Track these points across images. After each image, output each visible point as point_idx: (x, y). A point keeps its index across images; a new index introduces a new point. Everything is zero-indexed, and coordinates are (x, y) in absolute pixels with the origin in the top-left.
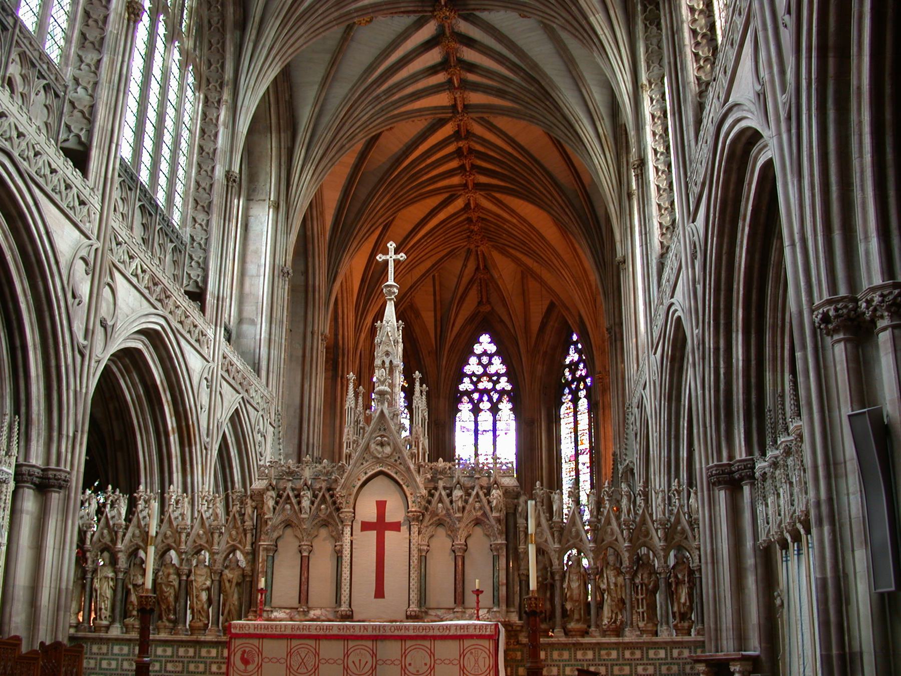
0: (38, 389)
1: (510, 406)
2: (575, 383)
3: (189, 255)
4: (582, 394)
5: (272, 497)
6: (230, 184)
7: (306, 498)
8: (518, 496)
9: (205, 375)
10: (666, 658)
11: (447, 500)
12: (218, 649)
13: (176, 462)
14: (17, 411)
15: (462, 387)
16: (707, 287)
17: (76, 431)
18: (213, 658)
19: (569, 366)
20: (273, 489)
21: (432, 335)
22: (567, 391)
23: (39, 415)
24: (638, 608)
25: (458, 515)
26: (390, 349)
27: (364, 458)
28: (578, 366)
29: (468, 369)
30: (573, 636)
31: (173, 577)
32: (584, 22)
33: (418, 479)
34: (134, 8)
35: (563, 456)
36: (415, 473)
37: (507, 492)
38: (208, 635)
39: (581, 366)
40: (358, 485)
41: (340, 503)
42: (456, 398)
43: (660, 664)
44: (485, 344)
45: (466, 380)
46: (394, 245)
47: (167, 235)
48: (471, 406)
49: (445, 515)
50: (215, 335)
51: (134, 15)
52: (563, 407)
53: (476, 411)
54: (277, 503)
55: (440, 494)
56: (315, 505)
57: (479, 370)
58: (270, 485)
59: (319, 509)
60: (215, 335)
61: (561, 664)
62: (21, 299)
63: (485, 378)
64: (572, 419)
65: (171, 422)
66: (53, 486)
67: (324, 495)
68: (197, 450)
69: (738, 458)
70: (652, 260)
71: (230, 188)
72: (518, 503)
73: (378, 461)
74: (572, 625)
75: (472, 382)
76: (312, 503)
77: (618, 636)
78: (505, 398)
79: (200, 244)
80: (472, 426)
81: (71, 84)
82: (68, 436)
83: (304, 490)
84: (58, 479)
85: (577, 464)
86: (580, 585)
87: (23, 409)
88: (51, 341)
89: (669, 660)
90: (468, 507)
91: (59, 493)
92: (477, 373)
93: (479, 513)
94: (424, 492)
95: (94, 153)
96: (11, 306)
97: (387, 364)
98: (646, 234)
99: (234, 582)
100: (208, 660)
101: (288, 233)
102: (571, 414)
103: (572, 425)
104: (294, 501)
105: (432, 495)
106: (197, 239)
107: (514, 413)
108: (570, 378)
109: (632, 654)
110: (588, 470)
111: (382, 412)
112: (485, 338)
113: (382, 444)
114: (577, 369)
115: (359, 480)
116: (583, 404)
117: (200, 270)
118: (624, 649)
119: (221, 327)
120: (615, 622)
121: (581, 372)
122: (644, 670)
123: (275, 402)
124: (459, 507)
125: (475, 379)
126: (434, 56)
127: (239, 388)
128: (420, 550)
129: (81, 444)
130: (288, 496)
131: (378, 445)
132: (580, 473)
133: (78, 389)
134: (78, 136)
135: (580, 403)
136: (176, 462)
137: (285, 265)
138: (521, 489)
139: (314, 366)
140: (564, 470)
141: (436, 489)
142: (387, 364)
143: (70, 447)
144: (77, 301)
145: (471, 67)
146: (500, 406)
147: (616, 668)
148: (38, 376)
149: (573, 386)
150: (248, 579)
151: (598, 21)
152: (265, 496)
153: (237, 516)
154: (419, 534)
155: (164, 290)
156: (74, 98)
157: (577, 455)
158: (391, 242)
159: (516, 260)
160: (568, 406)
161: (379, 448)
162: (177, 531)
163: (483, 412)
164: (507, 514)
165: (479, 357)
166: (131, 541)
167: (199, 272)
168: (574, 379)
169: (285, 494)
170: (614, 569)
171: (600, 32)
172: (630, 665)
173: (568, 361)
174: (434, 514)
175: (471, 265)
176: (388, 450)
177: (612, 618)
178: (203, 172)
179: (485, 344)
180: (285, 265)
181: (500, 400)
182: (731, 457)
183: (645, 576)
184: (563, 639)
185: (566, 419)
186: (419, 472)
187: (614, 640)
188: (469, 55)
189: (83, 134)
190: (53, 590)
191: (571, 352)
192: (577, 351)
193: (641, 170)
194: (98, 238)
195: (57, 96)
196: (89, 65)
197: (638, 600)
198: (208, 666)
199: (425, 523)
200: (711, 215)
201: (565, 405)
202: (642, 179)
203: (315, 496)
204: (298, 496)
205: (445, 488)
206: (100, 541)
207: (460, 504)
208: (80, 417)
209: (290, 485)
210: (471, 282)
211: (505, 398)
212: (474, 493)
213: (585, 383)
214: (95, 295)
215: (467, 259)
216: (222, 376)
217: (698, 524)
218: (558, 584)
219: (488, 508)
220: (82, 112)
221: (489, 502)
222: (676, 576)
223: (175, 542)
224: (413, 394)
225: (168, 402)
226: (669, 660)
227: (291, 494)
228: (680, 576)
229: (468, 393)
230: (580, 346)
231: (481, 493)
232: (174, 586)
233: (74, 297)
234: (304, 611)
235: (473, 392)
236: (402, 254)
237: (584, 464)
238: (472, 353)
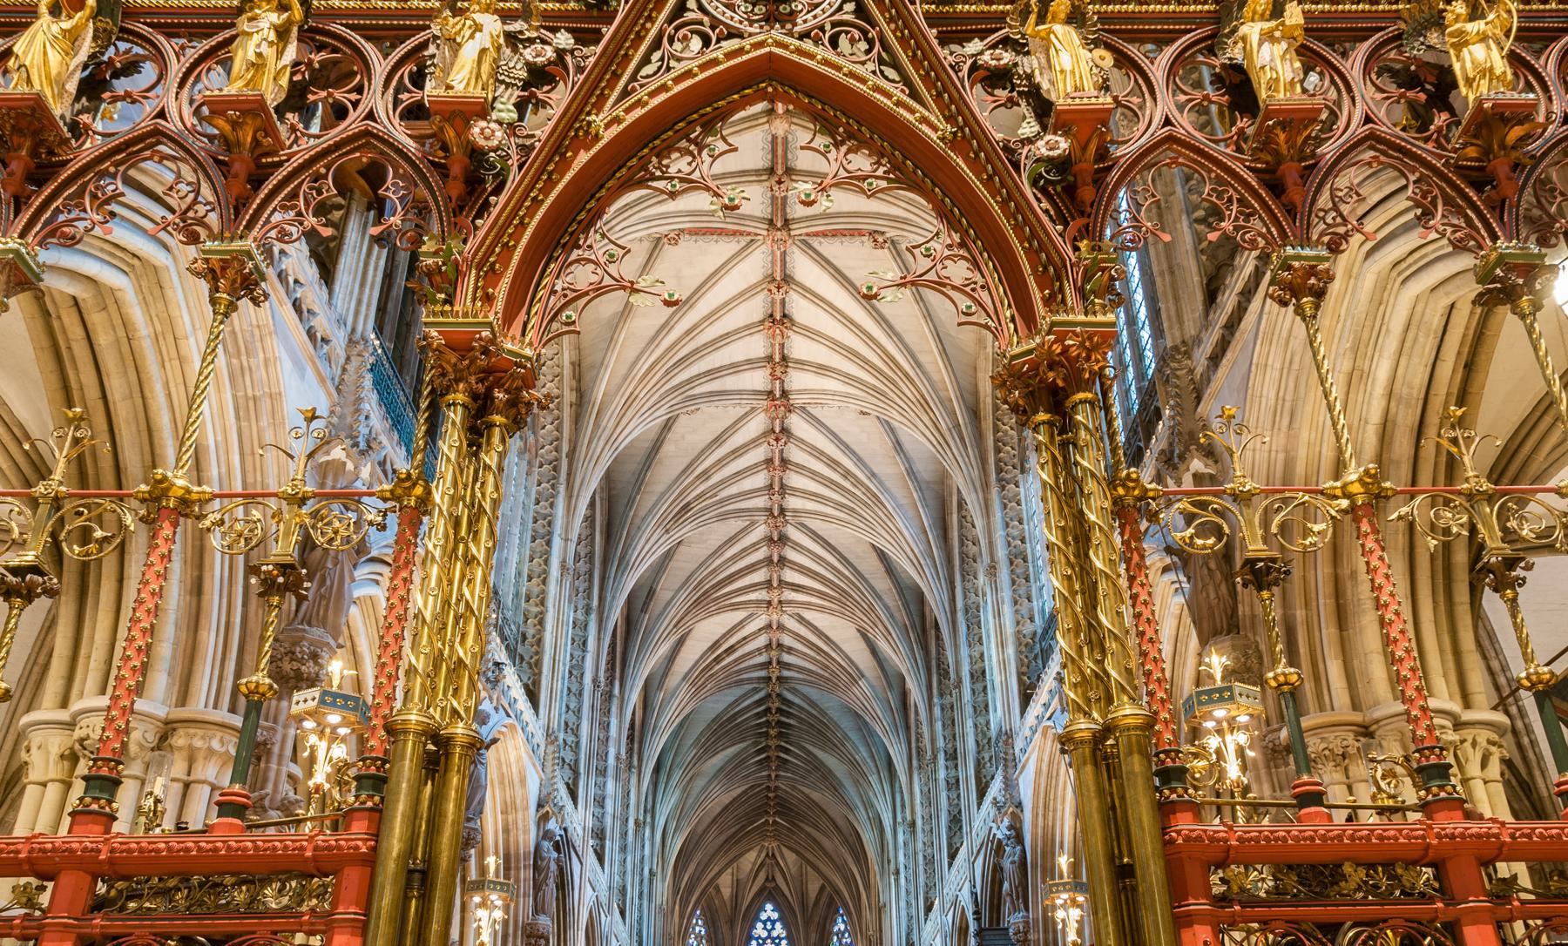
21: (728, 904)
44: (769, 911)
57: (764, 934)
101: (663, 880)
112: (769, 907)
151: (873, 779)
159: (798, 853)
173: (836, 929)
175: (763, 855)
179: (769, 911)
210: (762, 865)
215: (760, 852)
238: (757, 918)
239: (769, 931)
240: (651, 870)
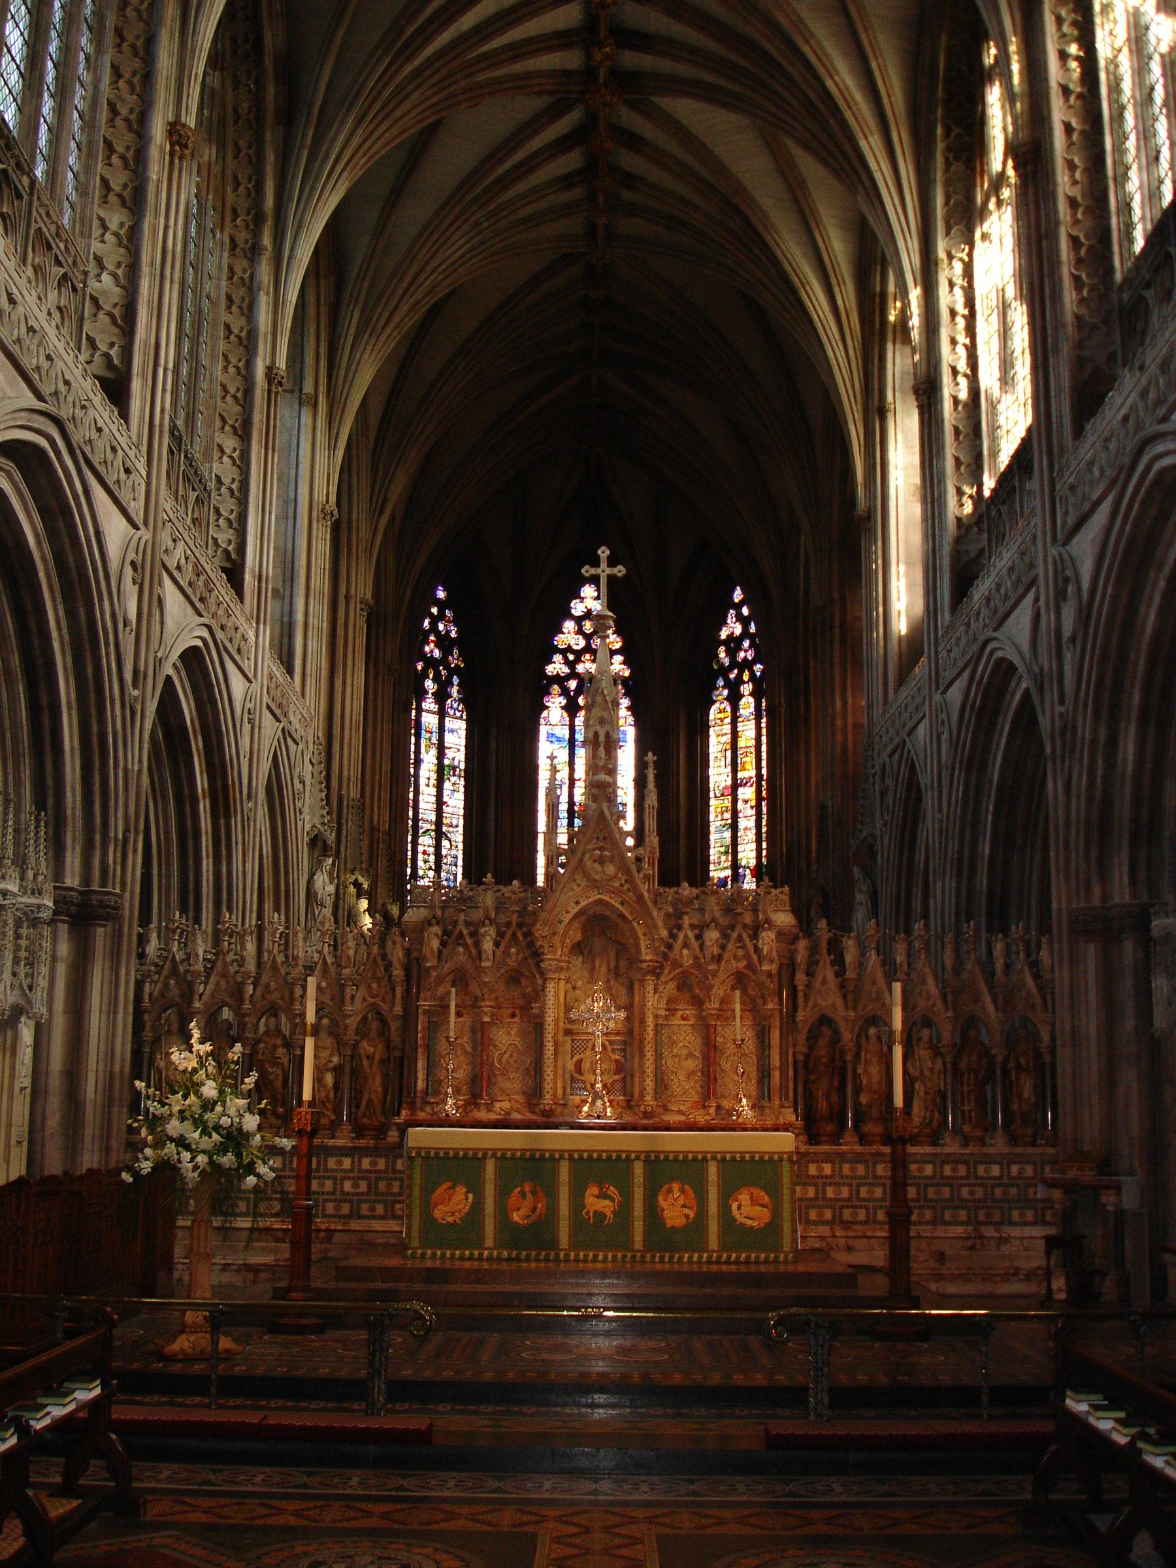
0: (73, 769)
2: (736, 671)
3: (215, 507)
4: (746, 689)
5: (436, 935)
6: (273, 388)
7: (488, 938)
8: (796, 938)
9: (248, 705)
10: (1001, 1177)
11: (695, 945)
12: (353, 1158)
13: (206, 842)
14: (40, 803)
15: (551, 669)
16: (1088, 653)
17: (126, 831)
18: (346, 1171)
20: (438, 923)
22: (721, 683)
23: (74, 808)
24: (963, 1104)
25: (713, 967)
26: (605, 715)
27: (575, 881)
28: (741, 644)
29: (561, 641)
30: (870, 1143)
31: (281, 1051)
32: (847, 147)
33: (655, 913)
34: (180, 135)
35: (711, 786)
36: (650, 904)
37: (779, 935)
38: (338, 1138)
39: (746, 644)
40: (566, 921)
41: (541, 947)
42: (542, 686)
43: (993, 1186)
45: (558, 658)
46: (608, 552)
47: (189, 480)
48: (564, 702)
49: (692, 966)
50: (257, 637)
51: (180, 145)
52: (713, 708)
53: (571, 709)
54: (443, 944)
55: (686, 936)
56: (502, 948)
58: (434, 917)
59: (507, 953)
60: (257, 637)
61: (855, 1182)
62: (54, 634)
63: (588, 656)
64: (727, 729)
65: (201, 782)
66: (97, 918)
67: (514, 934)
68: (236, 822)
69: (1117, 900)
70: (941, 545)
71: (273, 396)
72: (796, 950)
73: (594, 884)
74: (869, 1127)
75: (567, 662)
76: (497, 944)
77: (934, 1143)
79: (231, 490)
80: (565, 732)
81: (92, 268)
82: (116, 839)
83: (484, 925)
84: (108, 907)
85: (735, 801)
86: (880, 1070)
87: (50, 801)
88: (92, 697)
89: (1005, 1180)
90: (726, 956)
91: (105, 926)
92: (575, 647)
93: (742, 964)
94: (664, 933)
95: (136, 385)
96: (36, 642)
97: (602, 739)
98: (933, 502)
99: (377, 1057)
100: (339, 1175)
102: (728, 720)
103: (728, 738)
104: (469, 941)
105: (673, 936)
106: (226, 481)
107: (633, 715)
108: (727, 662)
109: (954, 1170)
110: (754, 812)
111: (602, 813)
113: (601, 861)
114: (739, 648)
115: (567, 912)
116: (747, 705)
117: (231, 531)
118: (943, 1163)
119: (265, 623)
120: (929, 1124)
121: (746, 653)
122: (971, 1193)
123: (314, 724)
124: (713, 956)
125: (571, 657)
126: (572, 160)
127: (278, 712)
128: (656, 1017)
129: (135, 851)
130: (461, 935)
131: (595, 861)
132: (741, 815)
133: (130, 766)
134: (107, 356)
135: (743, 702)
136: (206, 842)
137: (327, 502)
138: (801, 930)
139: (350, 650)
140: (712, 809)
141: (679, 927)
142: (602, 739)
143: (119, 855)
144: (128, 629)
145: (630, 180)
147: (931, 1190)
148: (72, 749)
149: (732, 676)
150: (396, 1053)
151: (871, 147)
152: (426, 935)
153: (379, 960)
154: (655, 993)
155: (209, 580)
156: (96, 291)
157: (736, 785)
158: (603, 548)
160: (722, 706)
161: (597, 866)
162: (286, 983)
164: (781, 965)
165: (579, 620)
166: (213, 996)
167: (230, 534)
168: (734, 664)
169: (456, 932)
170: (930, 1047)
171: (873, 166)
172: (951, 1185)
173: (724, 634)
174: (676, 964)
176: (610, 869)
177: (925, 1118)
178: (231, 369)
180: (327, 502)
182: (1104, 898)
183: (974, 1058)
184: (858, 1148)
185: (717, 728)
186: (655, 903)
187: (928, 1150)
188: (629, 161)
189: (113, 352)
190: (101, 1075)
191: (729, 621)
192: (740, 618)
193: (929, 399)
194: (146, 523)
195: (74, 289)
196: (116, 234)
197: (962, 1093)
198: (338, 1182)
199: (663, 979)
200: (1109, 555)
201: (717, 705)
202: (930, 412)
203: (501, 934)
204: (474, 934)
205: (692, 926)
206: (163, 996)
207: (716, 950)
208: (132, 809)
209: (462, 917)
212: (735, 935)
213: (752, 673)
214: (145, 617)
216: (268, 707)
217: (1053, 988)
218: (850, 1068)
219: (755, 957)
220: (111, 315)
221: (756, 948)
222: (1018, 1061)
223: (282, 998)
224: (645, 787)
225: (198, 750)
226: (1005, 1180)
227: (465, 932)
228: (1022, 1061)
229: (559, 680)
230: (745, 611)
231: (745, 936)
232: (282, 1064)
233: (125, 625)
234: (486, 1104)
235: (569, 677)
236: (620, 567)
237: (746, 802)
240: (270, 369)
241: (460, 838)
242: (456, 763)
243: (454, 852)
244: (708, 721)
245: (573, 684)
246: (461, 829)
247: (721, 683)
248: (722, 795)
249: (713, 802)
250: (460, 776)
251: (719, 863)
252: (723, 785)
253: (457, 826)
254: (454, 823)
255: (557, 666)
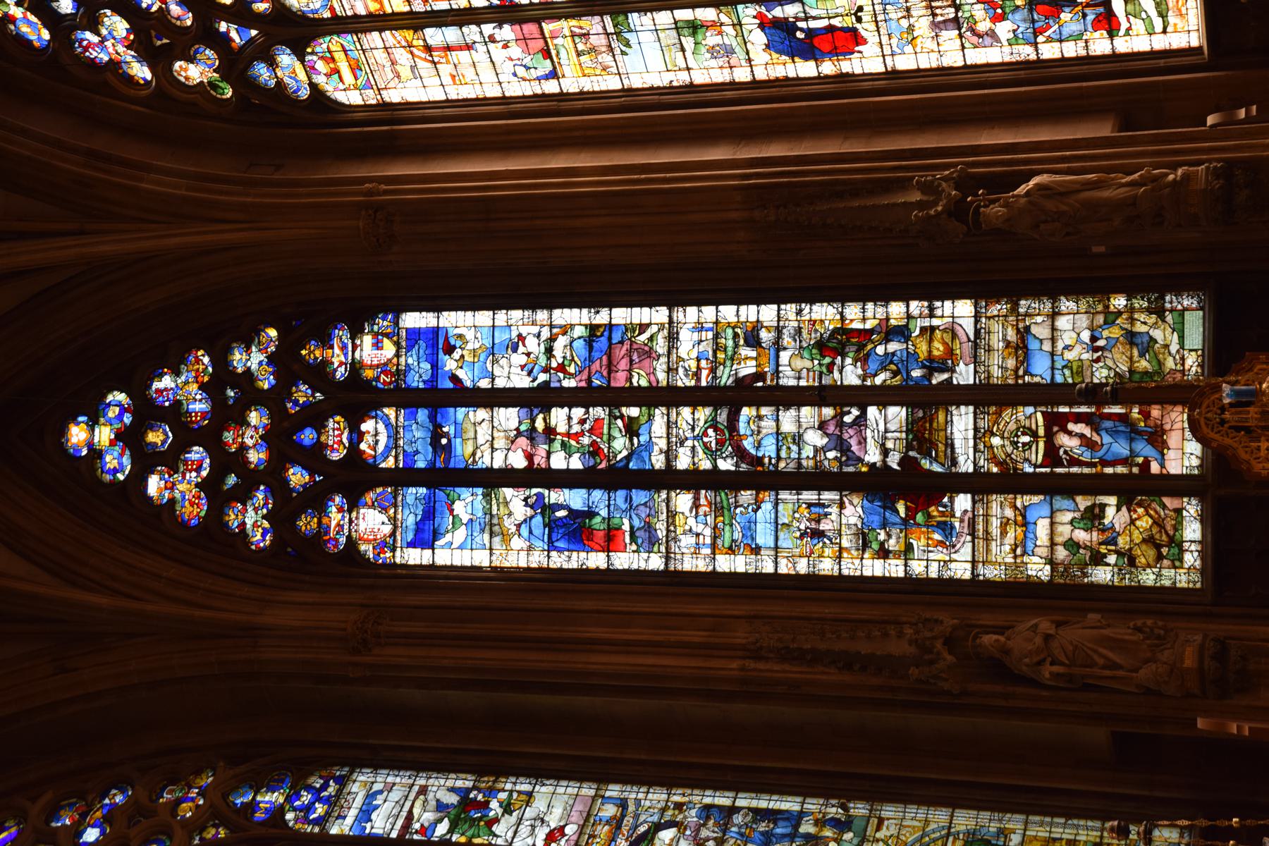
1: (342, 334)
2: (223, 26)
15: (259, 538)
19: (159, 59)
29: (193, 509)
35: (527, 89)
63: (228, 436)
75: (242, 495)
78: (310, 352)
102: (348, 40)
107: (372, 319)
125: (232, 480)
140: (588, 85)
146: (341, 373)
163: (363, 446)
165: (146, 461)
181: (319, 374)
201: (331, 88)
211: (310, 352)
229: (281, 518)
235: (279, 487)
239: (186, 434)
241: (657, 797)
242: (453, 799)
243: (692, 816)
244: (366, 107)
245: (297, 477)
246: (633, 794)
247: (262, 72)
248: (547, 54)
249: (571, 84)
250: (492, 792)
251: (729, 51)
252: (516, 51)
253: (623, 804)
254: (610, 811)
255: (250, 520)
